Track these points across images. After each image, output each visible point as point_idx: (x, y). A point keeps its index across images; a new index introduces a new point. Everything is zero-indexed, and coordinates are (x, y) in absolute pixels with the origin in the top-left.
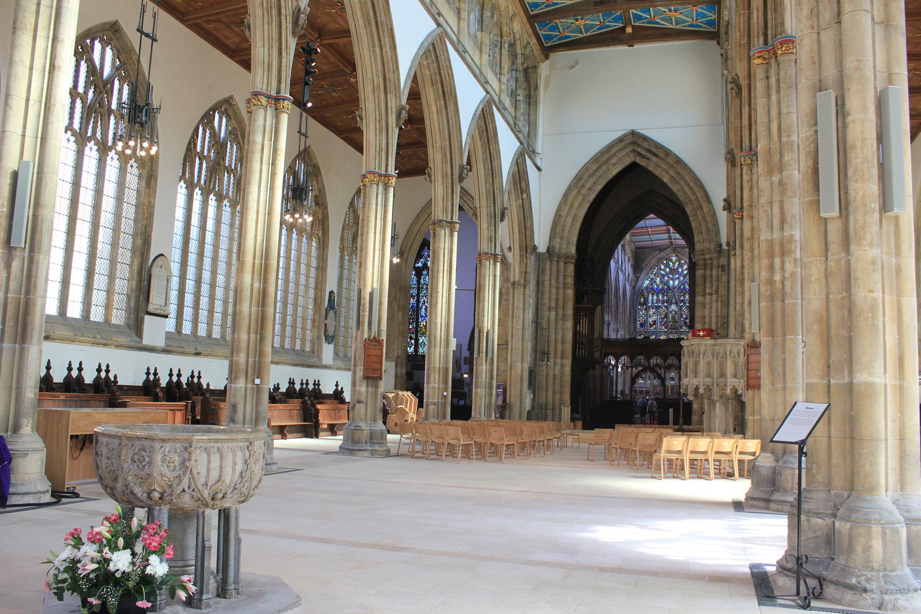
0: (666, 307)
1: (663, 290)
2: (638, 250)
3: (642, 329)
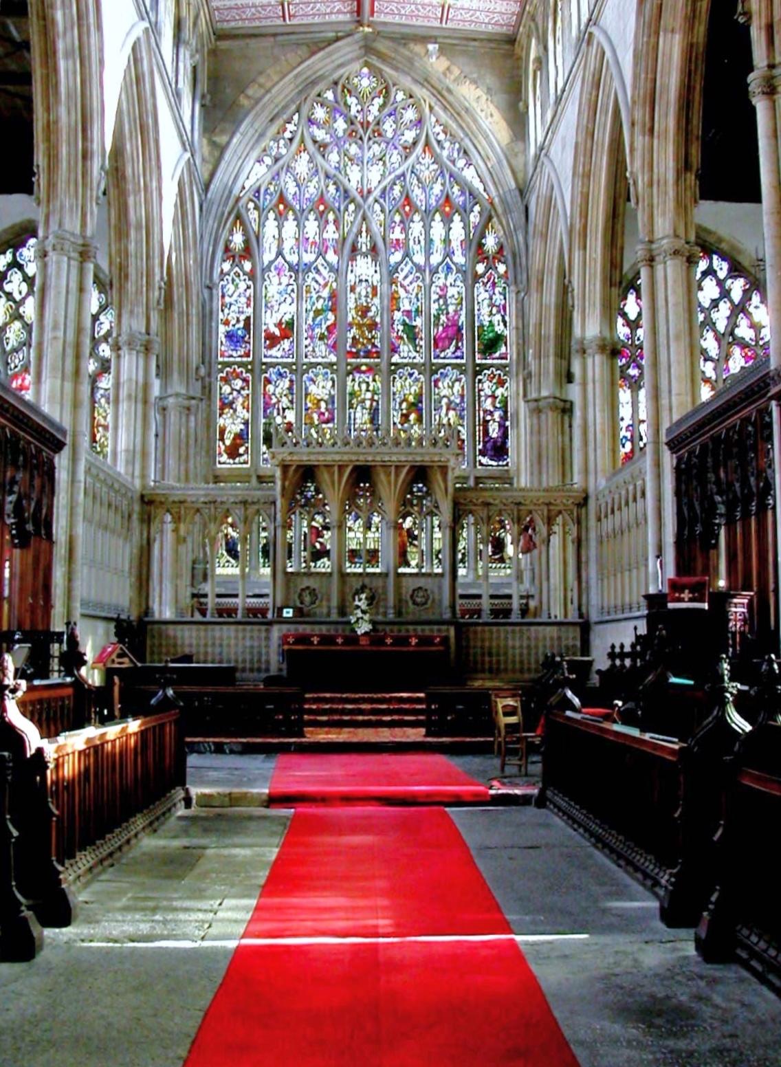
0: (332, 269)
1: (322, 200)
2: (224, 45)
3: (237, 355)
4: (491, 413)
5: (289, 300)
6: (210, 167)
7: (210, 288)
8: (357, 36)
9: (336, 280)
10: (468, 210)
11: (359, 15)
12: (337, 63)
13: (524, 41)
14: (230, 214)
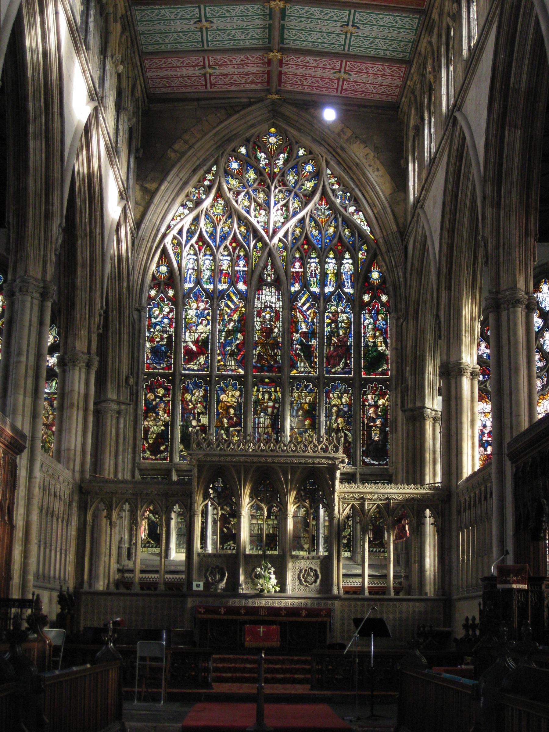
0: (242, 296)
3: (161, 368)
4: (374, 420)
5: (205, 322)
6: (142, 209)
7: (139, 311)
8: (267, 102)
9: (244, 307)
10: (357, 248)
11: (268, 85)
12: (250, 123)
13: (406, 108)
14: (157, 248)
